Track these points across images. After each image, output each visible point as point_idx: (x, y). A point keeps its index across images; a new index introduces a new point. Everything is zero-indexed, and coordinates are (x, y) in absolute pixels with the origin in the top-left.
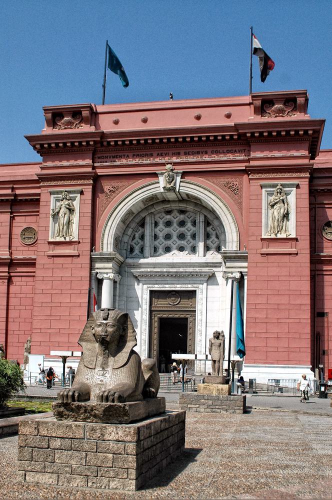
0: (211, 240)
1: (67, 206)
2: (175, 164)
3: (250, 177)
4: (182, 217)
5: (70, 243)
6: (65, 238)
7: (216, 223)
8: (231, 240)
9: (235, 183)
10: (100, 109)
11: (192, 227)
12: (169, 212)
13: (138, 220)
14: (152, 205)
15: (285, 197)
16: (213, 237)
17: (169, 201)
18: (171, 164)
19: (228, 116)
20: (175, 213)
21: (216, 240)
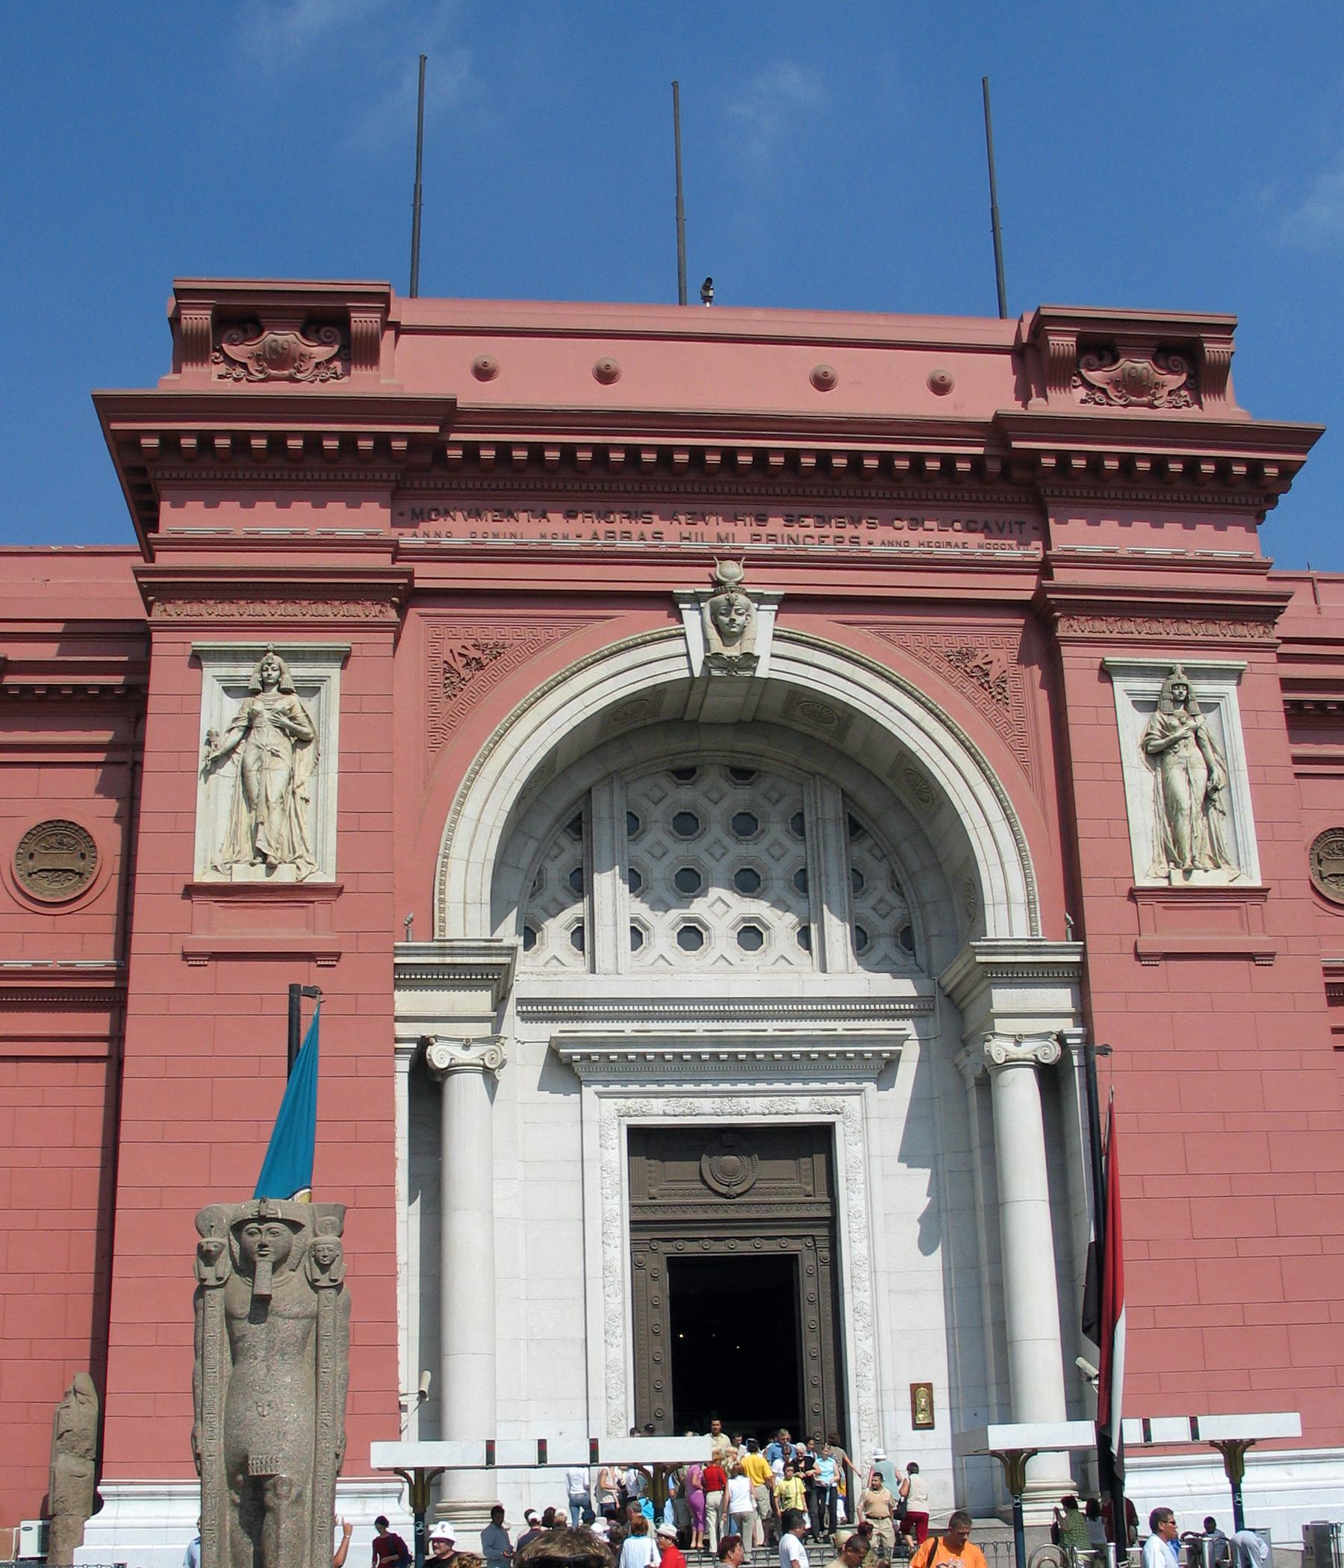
0: (871, 901)
1: (285, 720)
2: (754, 561)
3: (1062, 630)
4: (740, 797)
5: (299, 893)
6: (271, 868)
7: (895, 825)
8: (1001, 897)
9: (993, 655)
10: (403, 311)
11: (787, 842)
12: (685, 774)
13: (561, 800)
14: (624, 736)
15: (1200, 719)
16: (880, 887)
17: (695, 725)
18: (736, 558)
19: (940, 387)
20: (713, 779)
21: (892, 899)
